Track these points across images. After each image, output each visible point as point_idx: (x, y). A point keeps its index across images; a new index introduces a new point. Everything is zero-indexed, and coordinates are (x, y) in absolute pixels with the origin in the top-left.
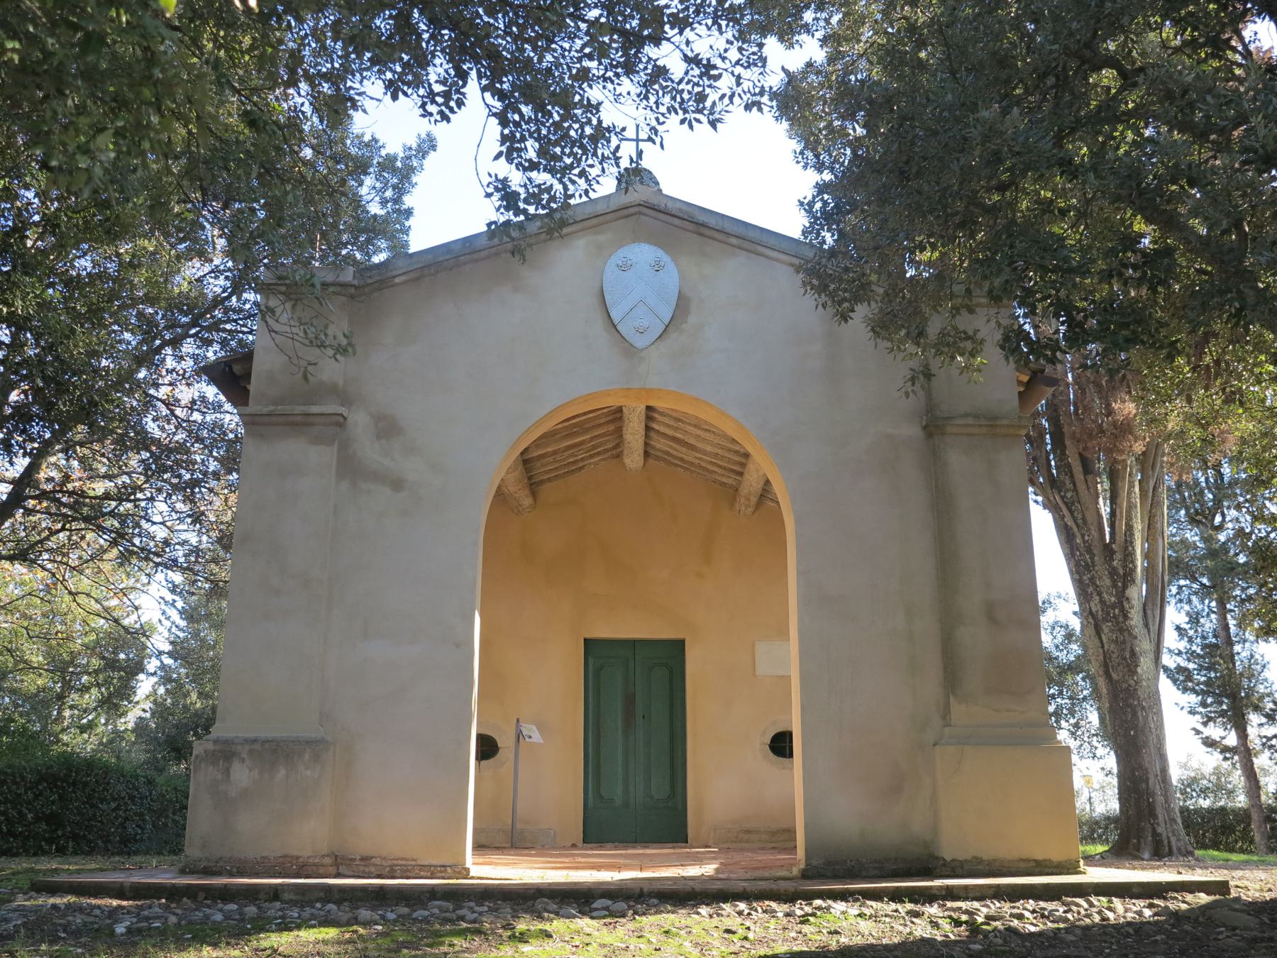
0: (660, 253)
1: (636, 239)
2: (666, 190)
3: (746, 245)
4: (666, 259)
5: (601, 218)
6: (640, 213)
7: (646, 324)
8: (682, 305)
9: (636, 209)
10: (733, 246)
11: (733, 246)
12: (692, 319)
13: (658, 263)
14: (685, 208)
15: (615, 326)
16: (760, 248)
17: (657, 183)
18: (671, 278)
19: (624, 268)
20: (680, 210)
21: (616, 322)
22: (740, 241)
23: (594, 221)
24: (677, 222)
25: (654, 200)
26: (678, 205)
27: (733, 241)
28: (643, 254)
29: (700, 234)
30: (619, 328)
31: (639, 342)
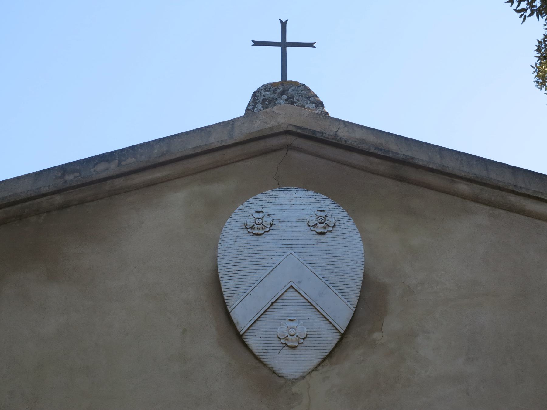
0: (326, 204)
1: (282, 182)
2: (334, 109)
3: (487, 193)
4: (337, 214)
5: (218, 156)
6: (289, 147)
7: (301, 331)
8: (371, 299)
9: (282, 140)
10: (463, 197)
11: (463, 197)
12: (392, 324)
13: (323, 220)
14: (371, 138)
15: (240, 337)
16: (513, 199)
17: (321, 104)
18: (349, 245)
19: (258, 229)
20: (363, 141)
21: (242, 326)
22: (477, 188)
23: (204, 160)
24: (356, 159)
25: (316, 126)
26: (358, 134)
27: (463, 187)
28: (294, 206)
29: (402, 179)
30: (249, 339)
31: (291, 366)
